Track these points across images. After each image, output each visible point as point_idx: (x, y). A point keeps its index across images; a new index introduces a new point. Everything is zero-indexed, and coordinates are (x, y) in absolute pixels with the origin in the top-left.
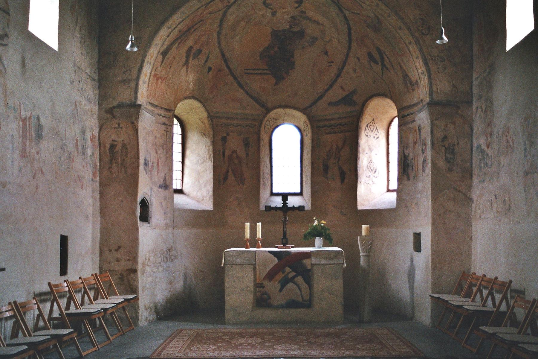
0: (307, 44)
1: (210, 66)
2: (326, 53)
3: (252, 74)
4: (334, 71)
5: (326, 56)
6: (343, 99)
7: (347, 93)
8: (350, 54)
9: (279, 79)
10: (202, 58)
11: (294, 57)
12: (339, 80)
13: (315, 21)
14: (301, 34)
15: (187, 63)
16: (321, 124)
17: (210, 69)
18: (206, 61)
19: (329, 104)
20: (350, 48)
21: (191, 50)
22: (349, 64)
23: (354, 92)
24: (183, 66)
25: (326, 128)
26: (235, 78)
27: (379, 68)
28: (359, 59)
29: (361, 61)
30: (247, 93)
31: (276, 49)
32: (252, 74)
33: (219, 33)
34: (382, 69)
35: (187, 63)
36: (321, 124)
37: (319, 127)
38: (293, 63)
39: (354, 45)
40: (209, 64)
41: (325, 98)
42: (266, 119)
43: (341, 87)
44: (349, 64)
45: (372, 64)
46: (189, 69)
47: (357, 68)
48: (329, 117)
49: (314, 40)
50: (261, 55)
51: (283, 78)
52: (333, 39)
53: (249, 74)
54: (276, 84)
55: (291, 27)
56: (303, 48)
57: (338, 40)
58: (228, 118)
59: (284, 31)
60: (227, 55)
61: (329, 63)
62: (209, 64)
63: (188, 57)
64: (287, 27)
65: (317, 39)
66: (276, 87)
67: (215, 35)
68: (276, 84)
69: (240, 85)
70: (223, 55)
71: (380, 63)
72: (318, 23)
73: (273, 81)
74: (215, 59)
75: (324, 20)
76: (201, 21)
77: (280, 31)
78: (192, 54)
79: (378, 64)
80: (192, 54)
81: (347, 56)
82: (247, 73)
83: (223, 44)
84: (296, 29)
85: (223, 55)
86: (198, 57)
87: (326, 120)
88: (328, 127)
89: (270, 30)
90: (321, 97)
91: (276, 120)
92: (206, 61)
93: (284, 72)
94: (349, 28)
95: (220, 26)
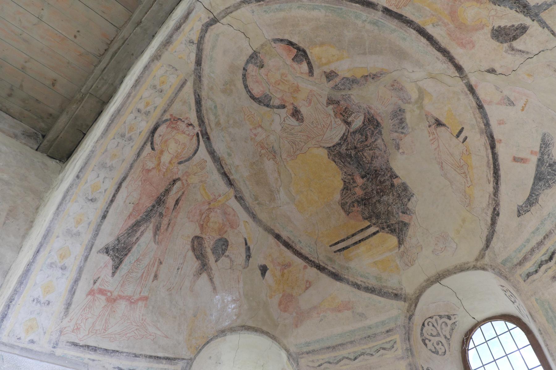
0: (395, 135)
1: (262, 262)
2: (439, 123)
3: (347, 248)
4: (478, 142)
5: (443, 128)
6: (539, 178)
7: (534, 159)
8: (473, 80)
9: (399, 230)
10: (237, 252)
11: (397, 177)
12: (500, 149)
13: (365, 77)
14: (372, 122)
15: (204, 267)
16: (529, 266)
17: (264, 270)
18: (249, 257)
19: (519, 214)
20: (459, 68)
21: (201, 244)
22: (490, 103)
23: (545, 144)
24: (199, 273)
25: (544, 267)
26: (320, 268)
27: (534, 27)
28: (492, 71)
29: (499, 71)
30: (358, 286)
31: (360, 181)
32: (347, 248)
33: (240, 198)
34: (543, 24)
35: (204, 267)
36: (529, 266)
37: (529, 275)
38: (405, 188)
39: (457, 52)
40: (258, 260)
41: (503, 210)
42: (418, 319)
43: (515, 159)
44: (490, 103)
45: (517, 44)
46: (217, 280)
47: (506, 93)
48: (533, 243)
49: (398, 115)
50: (343, 205)
51: (406, 225)
52: (420, 83)
53: (344, 249)
54: (401, 243)
55: (348, 124)
56: (398, 147)
57: (432, 77)
58: (334, 348)
59: (344, 138)
60: (284, 235)
61: (458, 136)
62: (258, 260)
63: (200, 255)
64: (342, 129)
65: (402, 111)
66: (402, 248)
67: (234, 204)
68: (401, 243)
69: (336, 276)
70: (278, 237)
71: (527, 21)
72: (374, 77)
73: (393, 240)
74: (266, 250)
75: (374, 63)
76: (175, 181)
77: (339, 144)
78: (209, 250)
79: (523, 29)
80: (209, 250)
81: (471, 89)
82: (339, 250)
83: (262, 216)
84: (358, 122)
85: (278, 237)
86: (227, 253)
87: (532, 250)
88: (546, 262)
89: (324, 153)
90: (496, 214)
91: (449, 318)
92: (249, 257)
93: (400, 214)
94: (422, 32)
95: (230, 183)
